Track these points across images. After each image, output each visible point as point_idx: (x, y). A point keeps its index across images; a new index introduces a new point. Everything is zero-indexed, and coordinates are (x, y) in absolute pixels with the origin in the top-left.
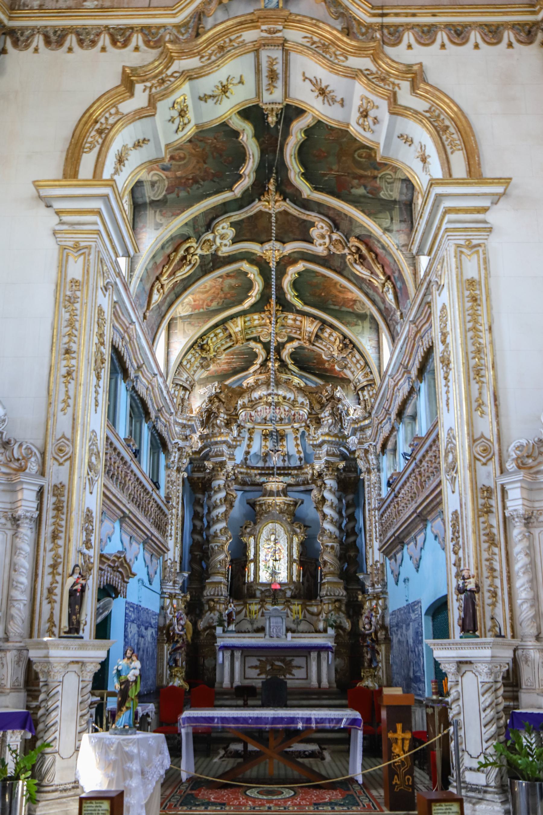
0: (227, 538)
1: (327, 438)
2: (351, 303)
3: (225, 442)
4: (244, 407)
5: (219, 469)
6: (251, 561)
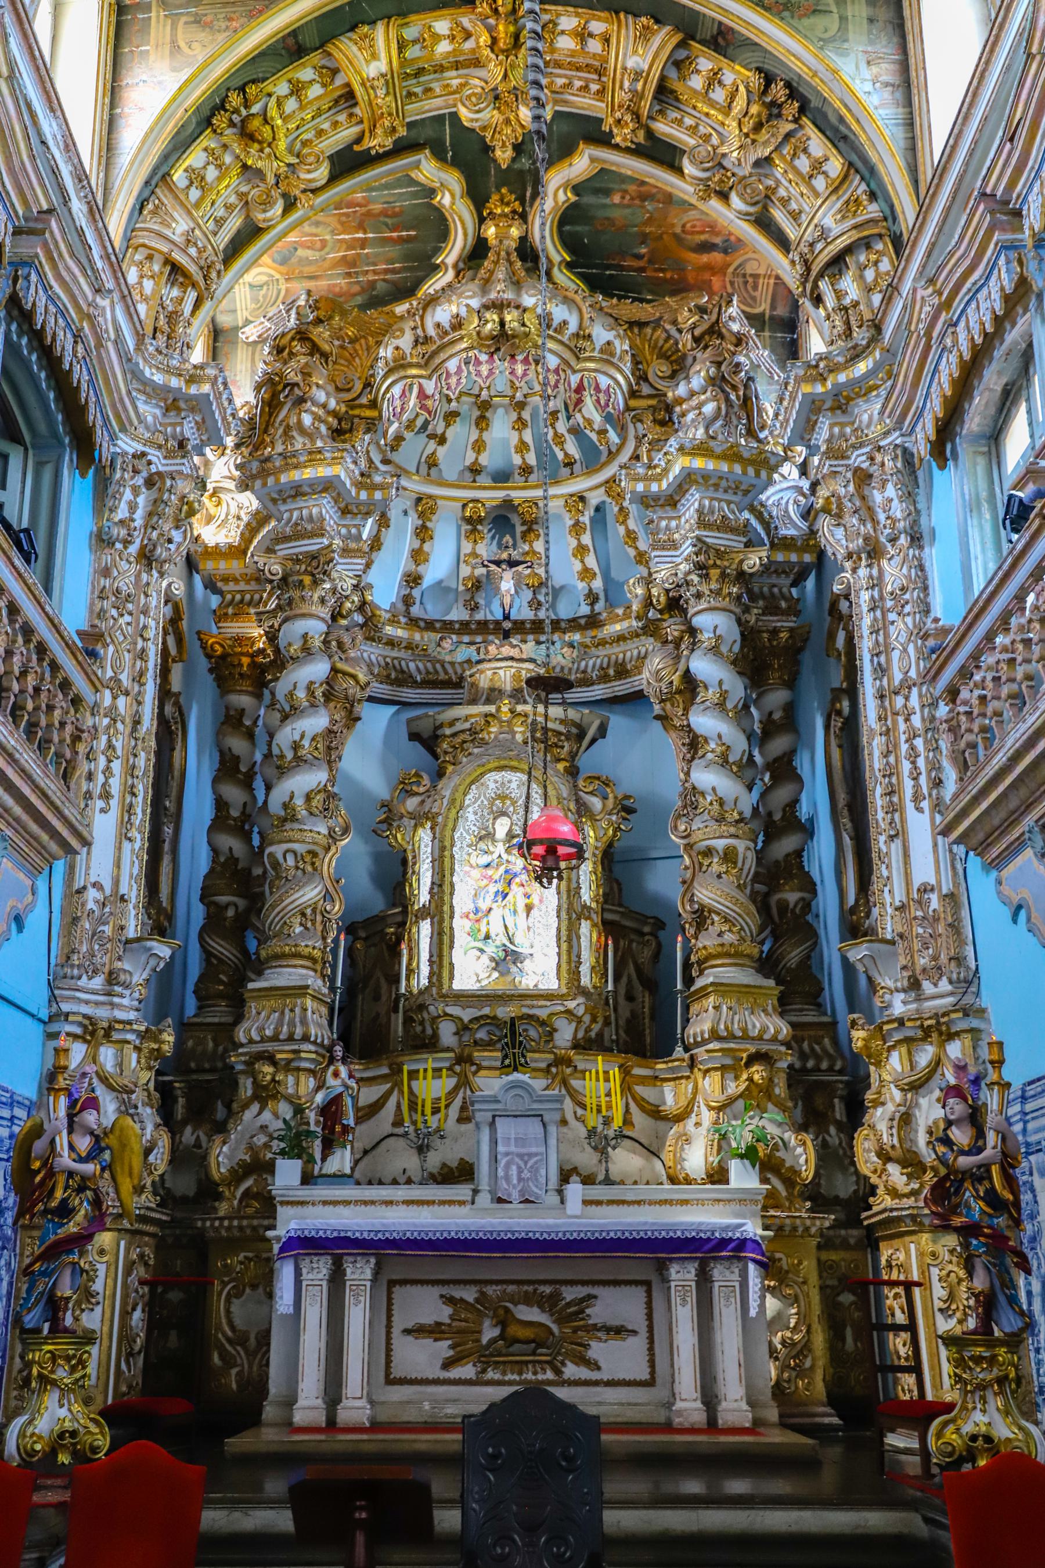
0: (331, 830)
1: (699, 463)
3: (328, 486)
4: (399, 365)
5: (307, 580)
6: (424, 913)
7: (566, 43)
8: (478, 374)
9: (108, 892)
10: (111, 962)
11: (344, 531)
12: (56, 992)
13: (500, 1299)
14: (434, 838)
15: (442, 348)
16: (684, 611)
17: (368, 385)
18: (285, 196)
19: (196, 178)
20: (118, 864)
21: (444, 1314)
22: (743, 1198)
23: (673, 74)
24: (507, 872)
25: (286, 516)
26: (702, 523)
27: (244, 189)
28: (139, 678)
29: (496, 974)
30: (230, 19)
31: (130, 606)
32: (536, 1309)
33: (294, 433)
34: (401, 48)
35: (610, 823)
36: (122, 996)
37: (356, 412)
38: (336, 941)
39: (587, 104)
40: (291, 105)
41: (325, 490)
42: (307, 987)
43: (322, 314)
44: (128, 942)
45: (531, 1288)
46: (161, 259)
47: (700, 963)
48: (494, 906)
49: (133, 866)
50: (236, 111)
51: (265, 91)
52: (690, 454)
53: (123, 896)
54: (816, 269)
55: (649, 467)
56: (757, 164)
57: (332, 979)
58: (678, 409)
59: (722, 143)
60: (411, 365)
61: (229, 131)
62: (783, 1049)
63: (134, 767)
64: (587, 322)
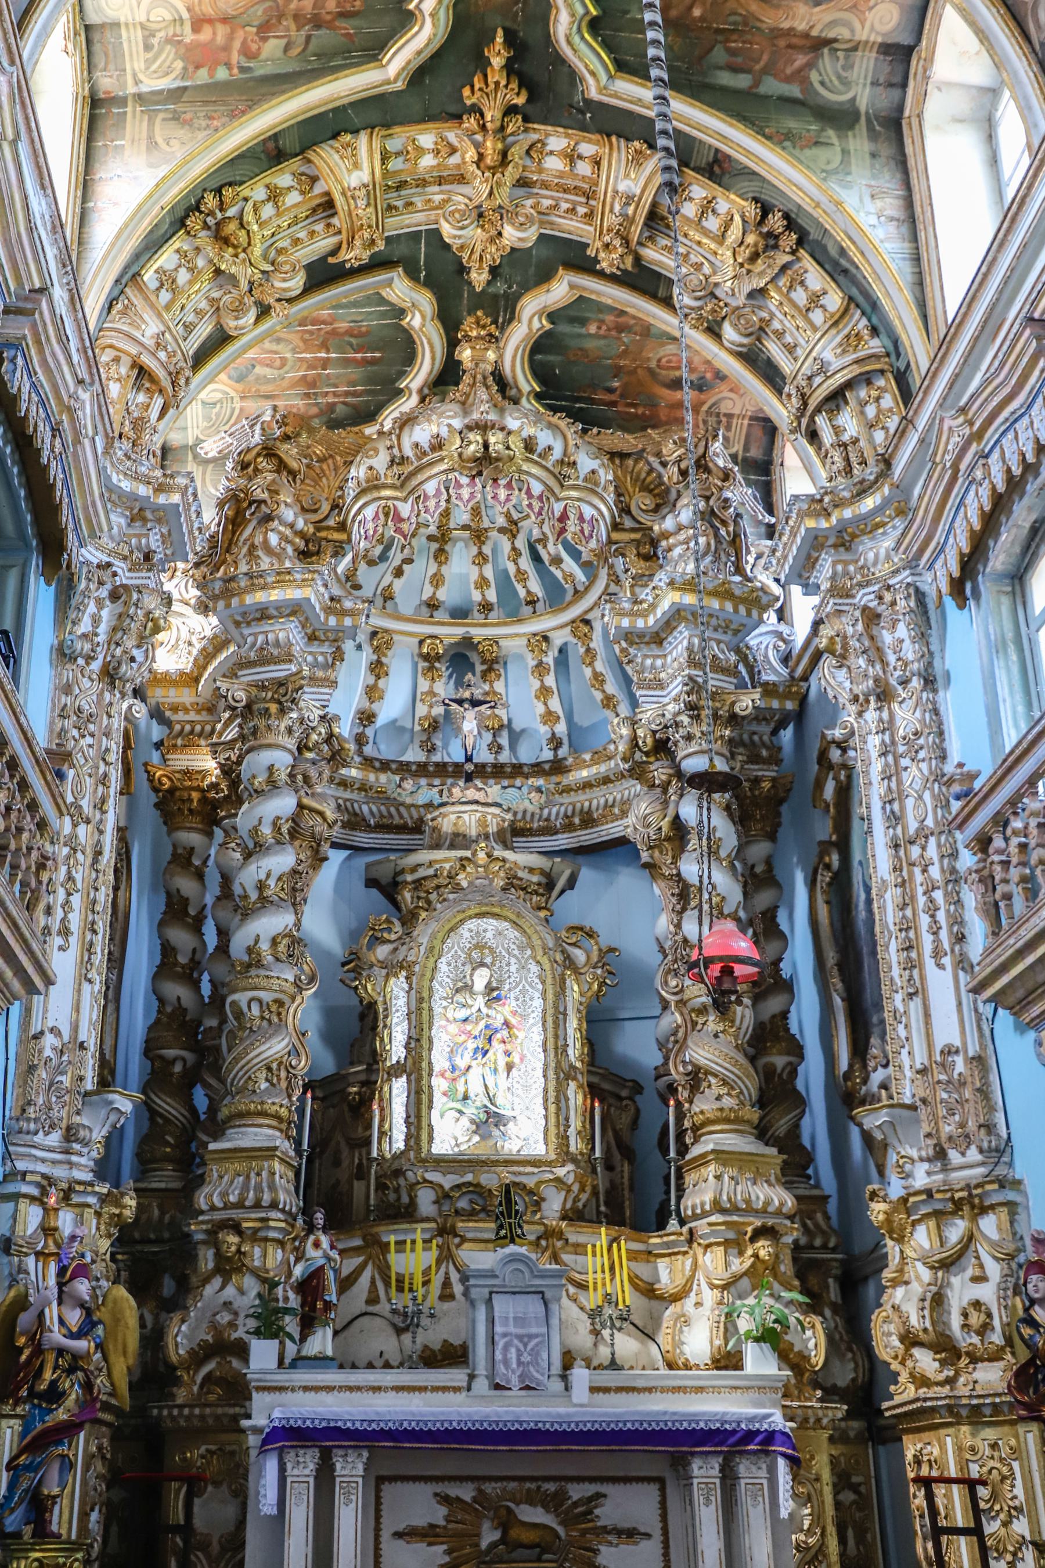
0: (298, 978)
1: (689, 599)
2: (801, 60)
3: (295, 609)
4: (372, 485)
5: (274, 708)
6: (397, 1070)
7: (554, 164)
8: (459, 497)
9: (66, 1039)
10: (69, 1117)
11: (310, 658)
12: (11, 1148)
13: (500, 1498)
14: (411, 988)
15: (419, 469)
16: (671, 755)
17: (336, 507)
18: (259, 304)
19: (166, 280)
20: (77, 1008)
21: (439, 1514)
22: (760, 1386)
23: (666, 200)
24: (487, 1027)
25: (250, 640)
26: (692, 663)
27: (216, 295)
28: (100, 805)
29: (476, 1138)
30: (211, 118)
31: (91, 727)
32: (540, 1510)
33: (260, 553)
34: (385, 158)
35: (596, 977)
36: (80, 1154)
37: (323, 534)
38: (302, 1099)
39: (573, 228)
40: (268, 211)
41: (294, 613)
42: (276, 1148)
43: (289, 430)
44: (87, 1094)
45: (533, 1486)
46: (126, 362)
47: (695, 1128)
48: (474, 1063)
49: (90, 1013)
50: (211, 213)
51: (242, 195)
52: (679, 589)
53: (82, 1044)
54: (813, 403)
55: (636, 602)
56: (751, 295)
57: (298, 1143)
58: (664, 543)
59: (715, 273)
60: (385, 486)
61: (203, 234)
62: (788, 1222)
63: (94, 902)
64: (571, 449)
